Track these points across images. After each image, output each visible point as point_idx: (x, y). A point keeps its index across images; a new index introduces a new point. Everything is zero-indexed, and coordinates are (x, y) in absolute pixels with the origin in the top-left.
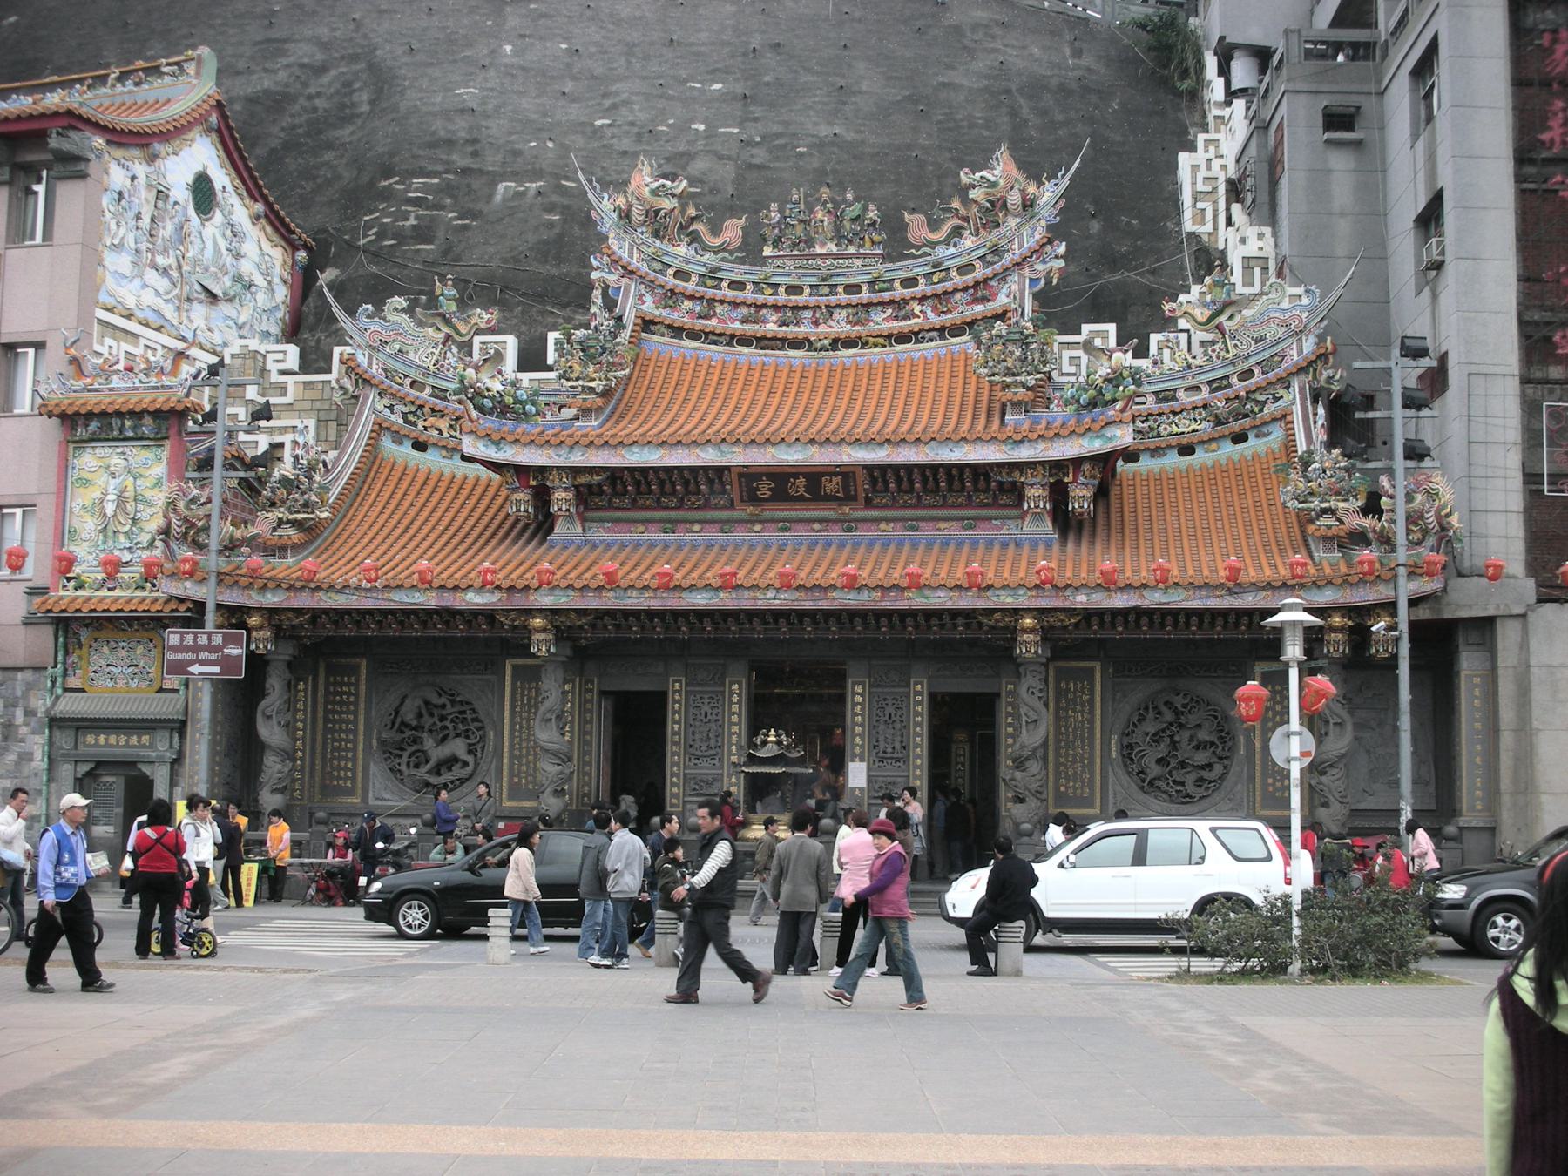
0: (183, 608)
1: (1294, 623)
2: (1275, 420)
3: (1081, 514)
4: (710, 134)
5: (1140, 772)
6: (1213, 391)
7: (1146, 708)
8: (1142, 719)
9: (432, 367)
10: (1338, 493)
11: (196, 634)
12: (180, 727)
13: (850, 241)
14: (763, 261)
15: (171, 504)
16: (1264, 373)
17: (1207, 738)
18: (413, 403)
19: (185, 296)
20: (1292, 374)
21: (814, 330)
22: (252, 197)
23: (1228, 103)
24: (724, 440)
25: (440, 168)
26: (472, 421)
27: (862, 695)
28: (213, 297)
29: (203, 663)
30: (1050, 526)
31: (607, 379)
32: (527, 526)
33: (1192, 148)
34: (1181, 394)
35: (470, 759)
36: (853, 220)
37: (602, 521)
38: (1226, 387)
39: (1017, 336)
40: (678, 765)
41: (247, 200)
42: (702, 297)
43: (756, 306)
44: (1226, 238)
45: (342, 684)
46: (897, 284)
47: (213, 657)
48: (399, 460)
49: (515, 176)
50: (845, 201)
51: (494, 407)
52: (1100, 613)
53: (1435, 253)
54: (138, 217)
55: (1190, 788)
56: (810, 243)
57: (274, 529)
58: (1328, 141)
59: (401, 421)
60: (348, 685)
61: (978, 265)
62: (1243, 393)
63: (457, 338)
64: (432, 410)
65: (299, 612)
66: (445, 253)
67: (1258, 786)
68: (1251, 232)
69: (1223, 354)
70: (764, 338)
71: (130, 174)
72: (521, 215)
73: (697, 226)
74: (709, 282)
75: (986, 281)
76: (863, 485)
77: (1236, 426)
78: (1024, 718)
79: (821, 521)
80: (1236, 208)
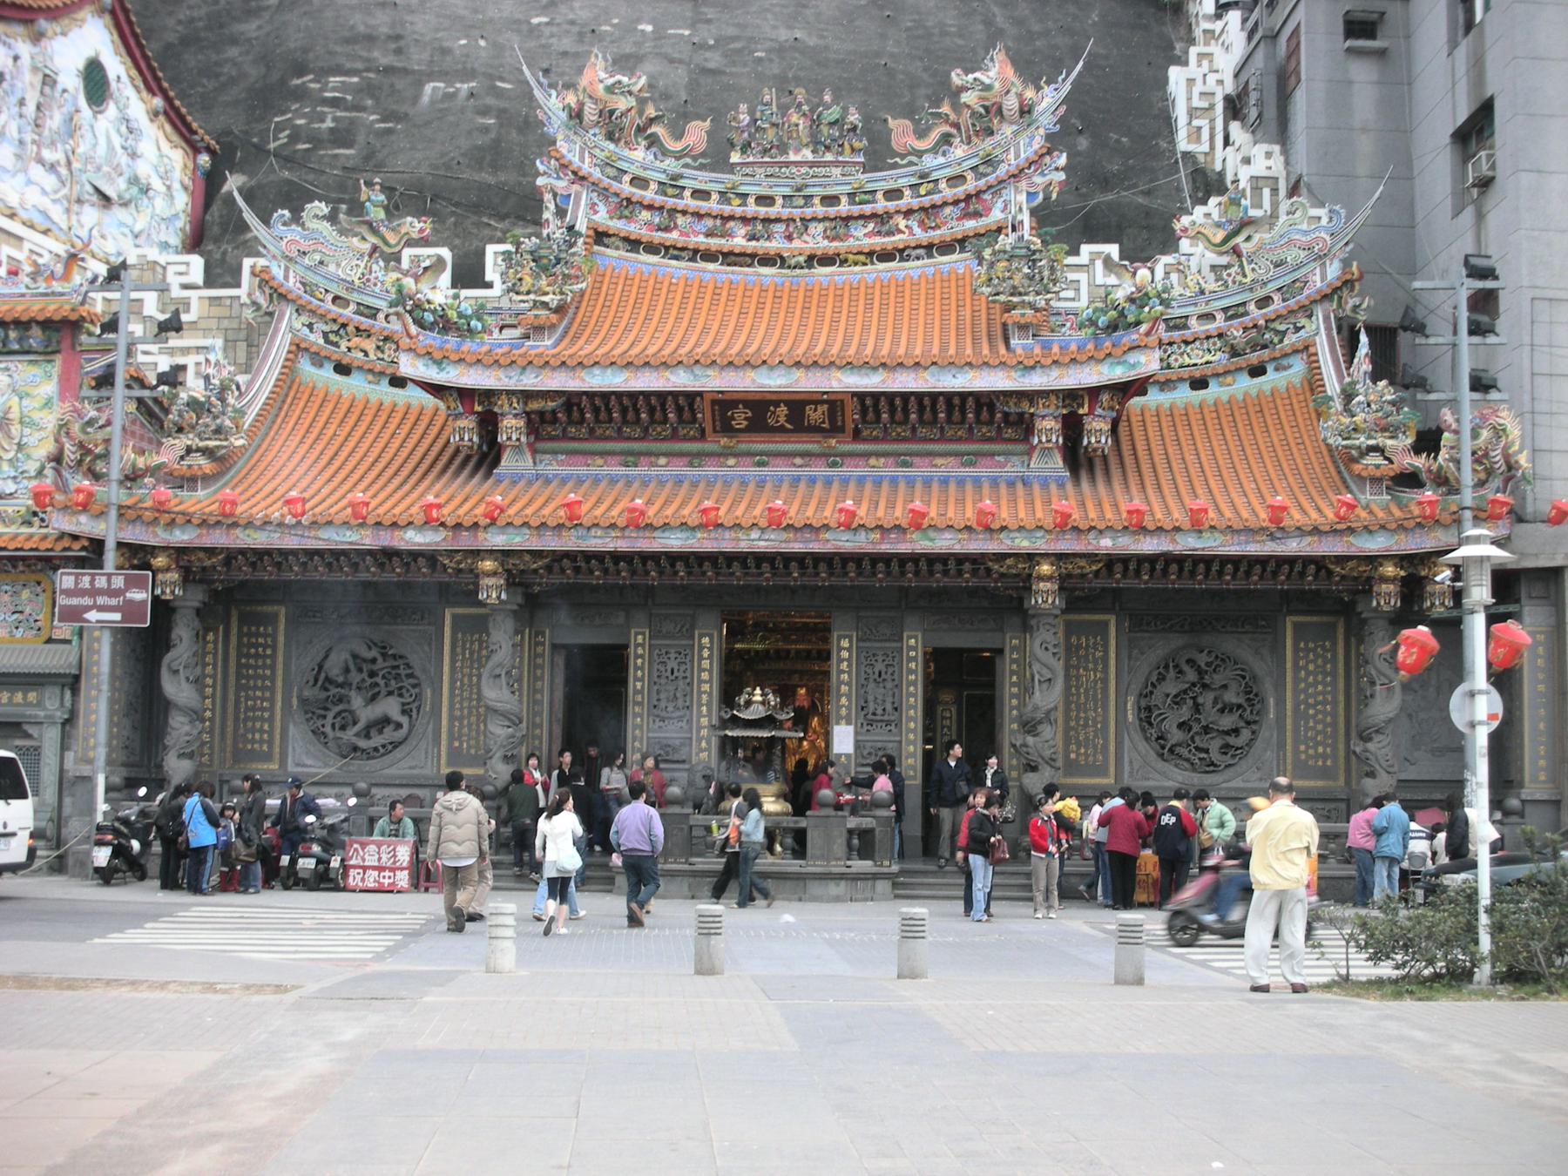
0: (76, 546)
1: (1482, 560)
2: (1296, 351)
3: (1095, 450)
4: (659, 35)
5: (1159, 738)
6: (1228, 319)
7: (1166, 667)
8: (1161, 678)
9: (357, 282)
10: (1384, 430)
11: (93, 575)
12: (73, 682)
13: (828, 148)
14: (731, 169)
15: (64, 428)
16: (1284, 300)
17: (1234, 700)
18: (335, 321)
19: (74, 197)
20: (1315, 302)
21: (787, 245)
22: (150, 89)
23: (1218, 16)
24: (697, 362)
25: (359, 65)
26: (411, 338)
27: (849, 650)
28: (105, 199)
29: (101, 609)
30: (1061, 464)
31: (562, 293)
32: (468, 458)
33: (1183, 61)
34: (1193, 322)
35: (404, 720)
36: (832, 124)
37: (555, 452)
38: (1242, 315)
39: (1023, 252)
40: (641, 727)
41: (145, 94)
42: (661, 208)
43: (722, 218)
44: (1227, 161)
45: (257, 635)
46: (879, 196)
47: (113, 602)
48: (320, 385)
49: (443, 75)
50: (821, 103)
51: (435, 323)
52: (1125, 560)
53: (1485, 167)
54: (22, 103)
55: (1215, 756)
56: (783, 148)
57: (182, 458)
58: (1349, 50)
59: (321, 341)
60: (265, 636)
61: (970, 176)
62: (1262, 322)
63: (386, 249)
64: (357, 329)
65: (211, 551)
66: (368, 158)
67: (1289, 754)
68: (1259, 151)
69: (1239, 278)
70: (731, 253)
71: (12, 53)
72: (451, 118)
73: (656, 129)
74: (670, 191)
75: (979, 193)
76: (852, 415)
77: (1254, 358)
78: (1037, 677)
79: (803, 455)
80: (1235, 127)
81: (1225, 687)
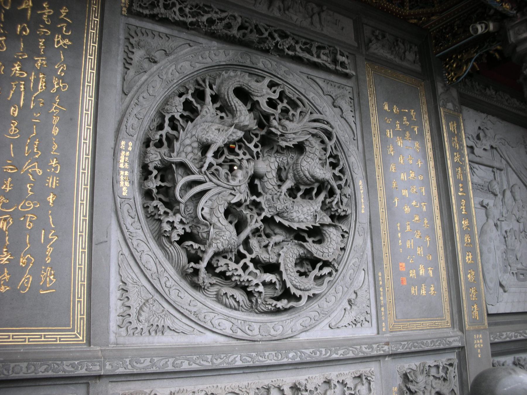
5: (185, 237)
7: (200, 95)
81: (300, 148)
